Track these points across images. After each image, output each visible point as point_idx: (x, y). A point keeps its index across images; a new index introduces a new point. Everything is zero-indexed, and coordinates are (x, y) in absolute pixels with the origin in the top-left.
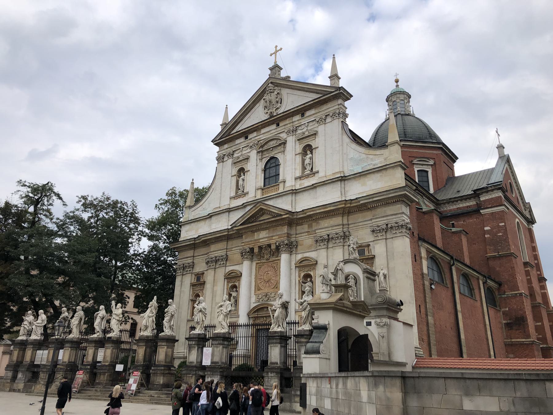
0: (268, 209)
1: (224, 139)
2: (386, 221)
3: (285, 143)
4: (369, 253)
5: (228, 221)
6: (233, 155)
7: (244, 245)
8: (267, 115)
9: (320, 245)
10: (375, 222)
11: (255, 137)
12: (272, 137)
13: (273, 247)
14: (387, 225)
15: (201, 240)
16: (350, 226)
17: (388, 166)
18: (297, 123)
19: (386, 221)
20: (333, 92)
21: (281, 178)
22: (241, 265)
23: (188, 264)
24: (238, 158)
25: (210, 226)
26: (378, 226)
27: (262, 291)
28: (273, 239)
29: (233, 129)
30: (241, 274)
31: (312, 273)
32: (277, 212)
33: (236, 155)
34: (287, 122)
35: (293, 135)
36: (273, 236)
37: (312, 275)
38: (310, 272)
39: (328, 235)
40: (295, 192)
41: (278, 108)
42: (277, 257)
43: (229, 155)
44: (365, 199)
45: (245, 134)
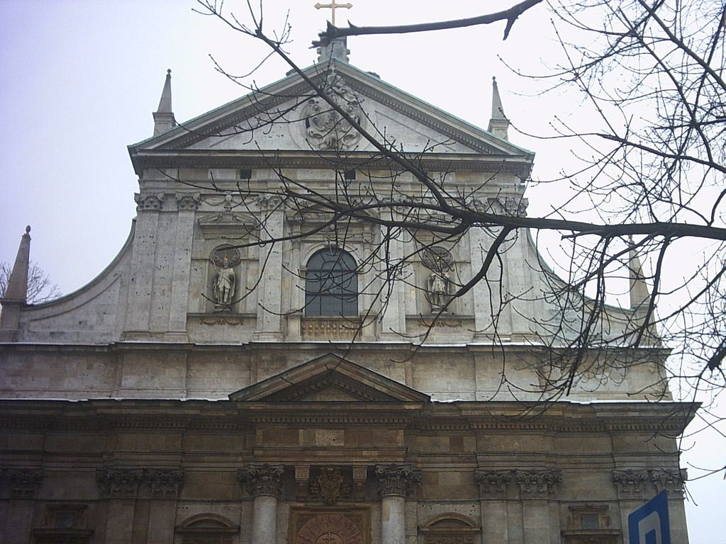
0: (357, 378)
1: (176, 155)
2: (644, 465)
4: (608, 524)
5: (187, 377)
6: (197, 203)
7: (263, 456)
8: (317, 141)
9: (489, 492)
10: (619, 462)
13: (359, 475)
14: (650, 472)
15: (92, 413)
18: (409, 188)
19: (644, 465)
20: (512, 156)
21: (364, 304)
23: (26, 471)
24: (220, 216)
26: (630, 472)
28: (362, 457)
30: (240, 528)
32: (384, 390)
33: (205, 207)
36: (362, 449)
39: (513, 472)
40: (413, 354)
41: (351, 136)
43: (188, 202)
44: (611, 410)
45: (247, 164)
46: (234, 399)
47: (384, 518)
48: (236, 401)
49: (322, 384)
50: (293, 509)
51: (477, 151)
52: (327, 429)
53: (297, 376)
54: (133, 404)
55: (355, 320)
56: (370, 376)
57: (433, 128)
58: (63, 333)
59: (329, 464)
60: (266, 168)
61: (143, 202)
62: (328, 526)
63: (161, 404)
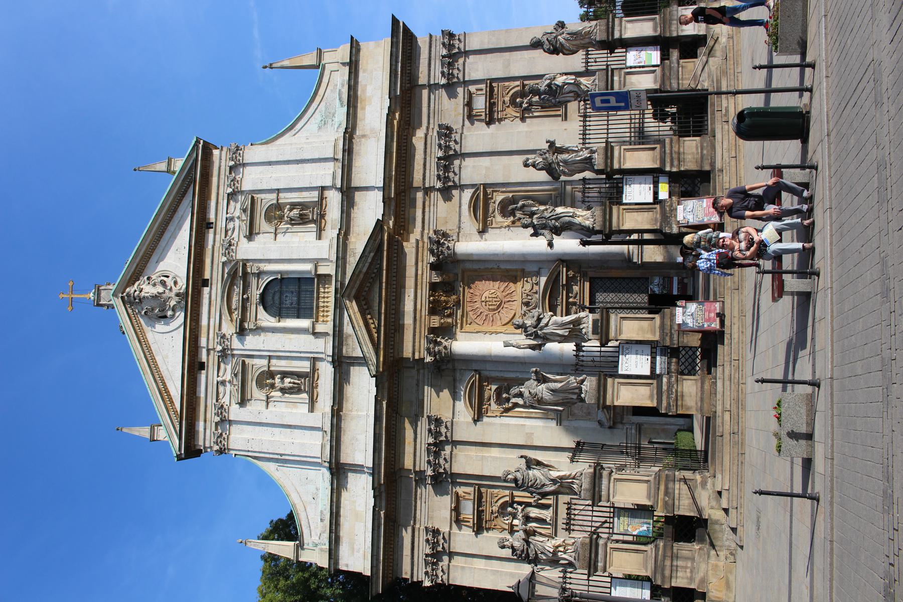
0: (362, 276)
3: (245, 262)
6: (222, 406)
7: (420, 352)
11: (208, 339)
12: (223, 292)
15: (383, 489)
16: (431, 126)
17: (353, 59)
18: (218, 236)
22: (458, 375)
25: (357, 469)
27: (517, 316)
28: (422, 274)
29: (172, 402)
31: (499, 197)
32: (372, 254)
33: (225, 400)
34: (208, 261)
35: (237, 245)
37: (503, 197)
38: (497, 203)
41: (176, 283)
42: (457, 275)
46: (374, 373)
47: (470, 259)
48: (377, 372)
49: (365, 305)
50: (462, 328)
51: (191, 183)
52: (400, 303)
53: (358, 324)
54: (377, 454)
55: (318, 280)
56: (361, 265)
57: (172, 217)
58: (321, 512)
59: (427, 300)
60: (198, 350)
61: (221, 449)
62: (476, 302)
63: (377, 432)
